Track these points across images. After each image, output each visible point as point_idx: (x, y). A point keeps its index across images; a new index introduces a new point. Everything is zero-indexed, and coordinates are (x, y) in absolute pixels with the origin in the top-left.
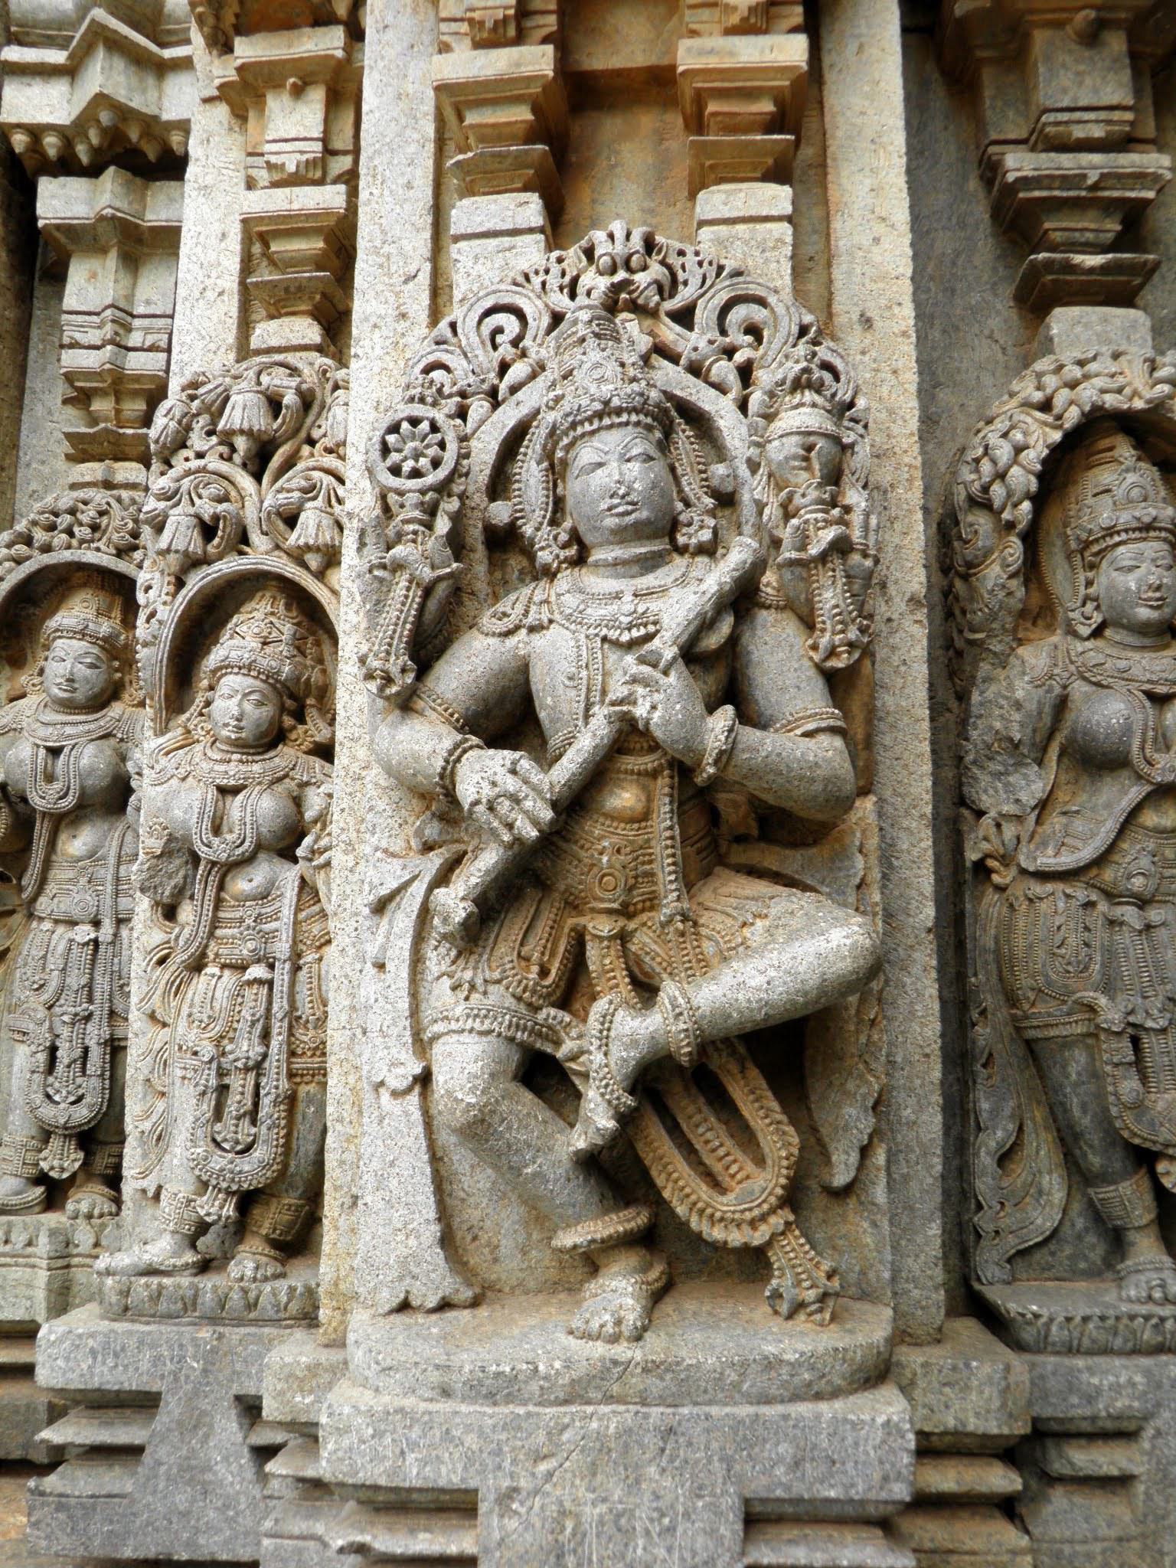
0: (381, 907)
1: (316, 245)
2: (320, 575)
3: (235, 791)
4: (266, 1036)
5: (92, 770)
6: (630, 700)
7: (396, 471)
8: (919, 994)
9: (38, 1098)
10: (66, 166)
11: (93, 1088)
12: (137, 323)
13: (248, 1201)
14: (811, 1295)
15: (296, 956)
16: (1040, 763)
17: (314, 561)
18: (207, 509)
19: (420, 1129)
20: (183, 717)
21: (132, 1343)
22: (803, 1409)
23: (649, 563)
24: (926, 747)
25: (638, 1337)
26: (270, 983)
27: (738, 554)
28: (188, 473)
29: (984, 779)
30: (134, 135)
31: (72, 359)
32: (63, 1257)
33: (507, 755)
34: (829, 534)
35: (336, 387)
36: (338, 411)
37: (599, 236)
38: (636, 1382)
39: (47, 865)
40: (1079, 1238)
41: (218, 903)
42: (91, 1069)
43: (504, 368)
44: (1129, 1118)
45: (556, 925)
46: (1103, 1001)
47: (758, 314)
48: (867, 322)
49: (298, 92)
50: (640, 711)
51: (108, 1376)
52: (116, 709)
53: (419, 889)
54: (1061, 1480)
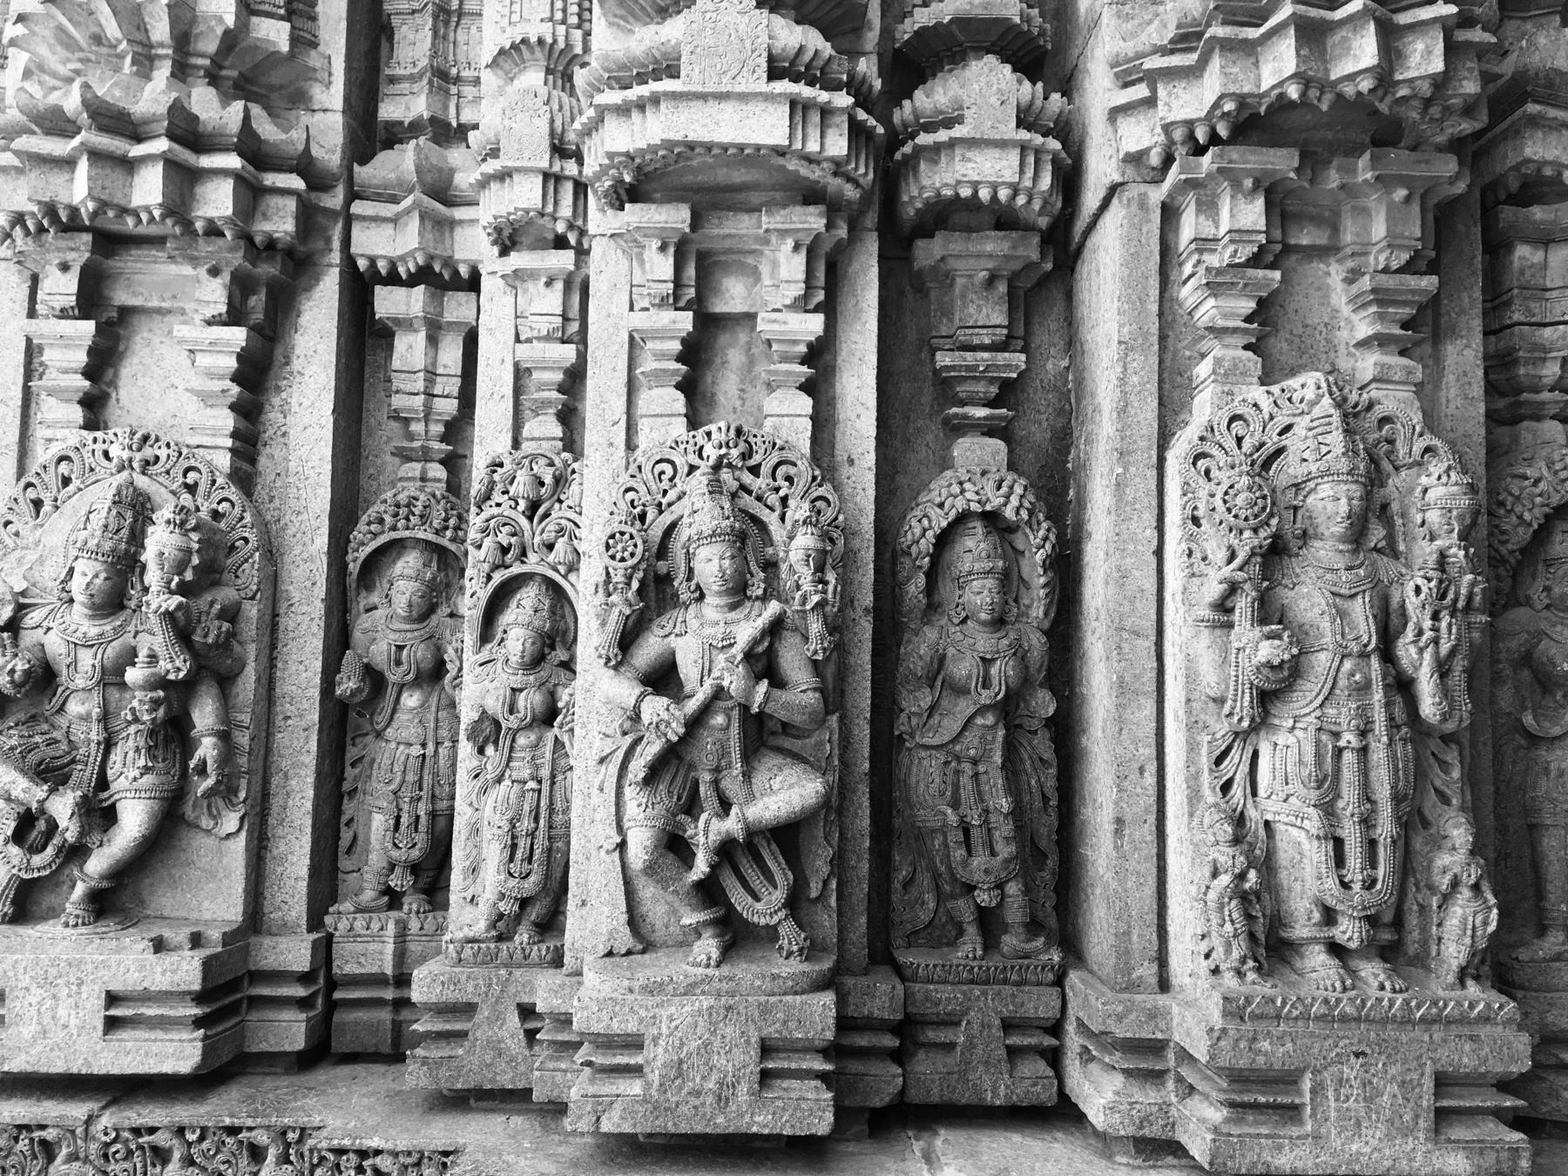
0: (602, 761)
1: (558, 377)
2: (565, 577)
3: (521, 690)
4: (537, 819)
5: (424, 658)
6: (721, 678)
7: (613, 557)
8: (860, 805)
9: (390, 846)
10: (393, 279)
11: (421, 838)
12: (439, 379)
13: (524, 903)
14: (795, 948)
15: (553, 776)
16: (932, 687)
17: (562, 569)
18: (504, 539)
19: (619, 869)
20: (489, 646)
21: (464, 978)
22: (789, 998)
23: (733, 607)
24: (869, 684)
25: (718, 966)
26: (540, 791)
27: (774, 607)
28: (493, 517)
29: (905, 693)
30: (437, 268)
31: (398, 401)
32: (402, 936)
33: (665, 701)
34: (816, 598)
35: (573, 472)
36: (575, 487)
37: (713, 428)
38: (716, 985)
39: (394, 711)
40: (943, 926)
41: (512, 749)
42: (421, 828)
43: (665, 492)
44: (960, 869)
45: (686, 776)
46: (949, 811)
47: (792, 471)
48: (851, 462)
49: (549, 284)
50: (725, 684)
51: (451, 995)
52: (434, 619)
53: (620, 754)
54: (924, 1045)
